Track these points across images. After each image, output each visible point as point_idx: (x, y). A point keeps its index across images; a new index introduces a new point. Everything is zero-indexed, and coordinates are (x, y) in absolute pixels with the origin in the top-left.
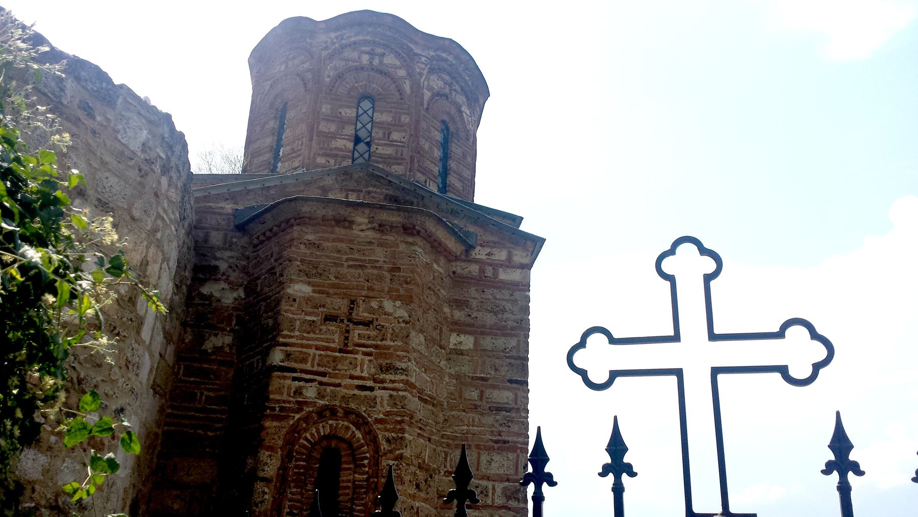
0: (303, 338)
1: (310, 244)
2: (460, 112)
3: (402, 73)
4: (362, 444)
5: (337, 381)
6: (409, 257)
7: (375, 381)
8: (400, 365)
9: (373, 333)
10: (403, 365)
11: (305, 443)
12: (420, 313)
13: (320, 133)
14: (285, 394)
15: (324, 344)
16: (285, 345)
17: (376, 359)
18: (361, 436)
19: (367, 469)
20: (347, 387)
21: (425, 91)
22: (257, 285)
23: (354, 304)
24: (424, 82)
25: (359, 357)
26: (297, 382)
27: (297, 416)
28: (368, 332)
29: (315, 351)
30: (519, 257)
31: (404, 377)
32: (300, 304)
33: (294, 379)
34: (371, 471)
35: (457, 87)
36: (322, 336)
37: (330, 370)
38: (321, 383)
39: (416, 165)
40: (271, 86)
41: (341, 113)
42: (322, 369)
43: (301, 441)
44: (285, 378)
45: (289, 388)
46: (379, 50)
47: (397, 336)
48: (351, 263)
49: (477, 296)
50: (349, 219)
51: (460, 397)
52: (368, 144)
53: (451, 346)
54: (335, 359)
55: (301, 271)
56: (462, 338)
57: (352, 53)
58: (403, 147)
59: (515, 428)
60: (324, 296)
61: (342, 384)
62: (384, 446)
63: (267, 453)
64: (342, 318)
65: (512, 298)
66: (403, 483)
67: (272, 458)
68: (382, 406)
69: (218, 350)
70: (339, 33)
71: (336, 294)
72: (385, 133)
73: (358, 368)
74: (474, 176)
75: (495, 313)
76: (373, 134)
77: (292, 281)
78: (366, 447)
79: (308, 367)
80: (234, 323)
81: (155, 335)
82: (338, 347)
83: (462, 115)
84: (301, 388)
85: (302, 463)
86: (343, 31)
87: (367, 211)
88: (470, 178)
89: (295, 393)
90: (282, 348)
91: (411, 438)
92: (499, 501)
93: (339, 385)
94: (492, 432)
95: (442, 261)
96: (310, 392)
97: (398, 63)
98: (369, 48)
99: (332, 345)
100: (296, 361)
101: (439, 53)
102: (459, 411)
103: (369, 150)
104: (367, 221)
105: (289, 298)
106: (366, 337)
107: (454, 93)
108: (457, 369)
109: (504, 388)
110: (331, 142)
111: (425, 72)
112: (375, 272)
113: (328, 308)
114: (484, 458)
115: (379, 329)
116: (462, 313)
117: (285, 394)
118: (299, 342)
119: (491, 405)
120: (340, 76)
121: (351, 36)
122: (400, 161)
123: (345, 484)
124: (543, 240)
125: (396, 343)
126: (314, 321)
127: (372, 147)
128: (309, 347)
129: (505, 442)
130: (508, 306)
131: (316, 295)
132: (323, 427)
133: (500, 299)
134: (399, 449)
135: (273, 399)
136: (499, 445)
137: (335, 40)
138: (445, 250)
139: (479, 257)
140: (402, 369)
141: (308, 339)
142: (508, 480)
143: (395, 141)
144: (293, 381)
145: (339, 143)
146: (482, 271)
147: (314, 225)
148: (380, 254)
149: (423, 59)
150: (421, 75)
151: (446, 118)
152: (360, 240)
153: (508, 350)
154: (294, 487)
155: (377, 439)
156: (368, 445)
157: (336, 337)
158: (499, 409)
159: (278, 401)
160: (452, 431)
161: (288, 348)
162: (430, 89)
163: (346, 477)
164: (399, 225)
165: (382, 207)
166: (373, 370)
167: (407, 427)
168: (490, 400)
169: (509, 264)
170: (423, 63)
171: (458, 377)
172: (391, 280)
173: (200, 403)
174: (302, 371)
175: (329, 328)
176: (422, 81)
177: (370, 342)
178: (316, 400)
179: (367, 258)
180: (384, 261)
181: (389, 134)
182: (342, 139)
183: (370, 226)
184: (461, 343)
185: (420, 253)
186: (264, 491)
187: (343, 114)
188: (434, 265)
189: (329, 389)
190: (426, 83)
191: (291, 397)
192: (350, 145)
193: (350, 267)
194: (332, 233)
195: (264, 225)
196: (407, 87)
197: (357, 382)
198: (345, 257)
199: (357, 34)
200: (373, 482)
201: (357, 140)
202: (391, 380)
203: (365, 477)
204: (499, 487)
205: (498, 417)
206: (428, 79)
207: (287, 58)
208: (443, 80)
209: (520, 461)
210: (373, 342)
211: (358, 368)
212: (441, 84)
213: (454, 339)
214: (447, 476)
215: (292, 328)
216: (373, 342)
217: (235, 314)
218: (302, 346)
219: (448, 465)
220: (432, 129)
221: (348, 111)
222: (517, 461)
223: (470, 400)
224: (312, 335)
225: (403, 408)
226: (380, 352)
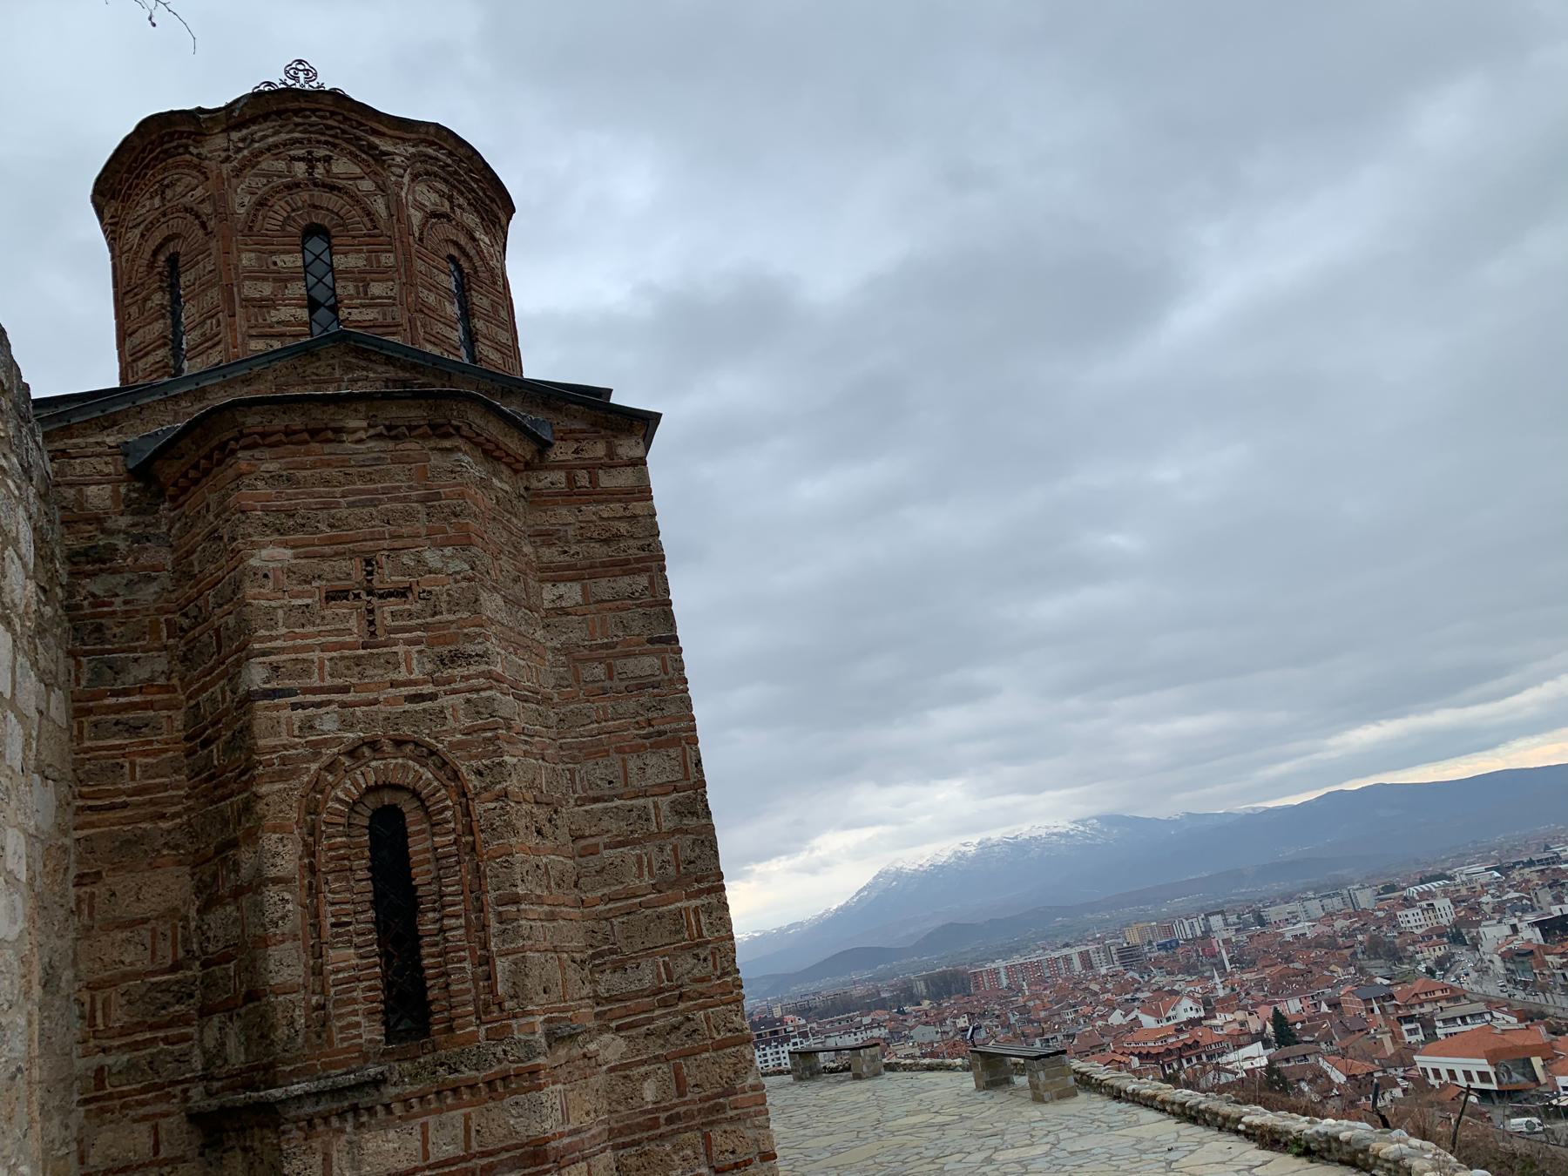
0: (295, 636)
1: (275, 478)
2: (474, 239)
4: (435, 787)
5: (372, 696)
6: (452, 472)
7: (435, 683)
8: (470, 648)
9: (417, 607)
10: (479, 649)
11: (337, 806)
12: (487, 560)
13: (248, 302)
14: (284, 734)
15: (334, 639)
16: (264, 653)
17: (431, 646)
18: (430, 776)
19: (452, 825)
20: (391, 702)
21: (412, 211)
22: (191, 564)
23: (372, 565)
24: (406, 198)
25: (400, 649)
26: (300, 711)
27: (314, 767)
28: (408, 607)
29: (322, 654)
30: (627, 449)
31: (484, 667)
32: (276, 580)
33: (294, 706)
34: (459, 827)
36: (329, 627)
37: (354, 681)
38: (343, 705)
39: (421, 331)
40: (142, 236)
41: (275, 263)
42: (339, 682)
43: (330, 804)
44: (277, 708)
45: (289, 723)
46: (322, 152)
47: (458, 604)
48: (351, 499)
49: (571, 520)
50: (332, 425)
51: (578, 681)
52: (334, 309)
53: (547, 605)
54: (358, 661)
55: (266, 525)
56: (562, 588)
57: (275, 163)
58: (394, 304)
59: (672, 709)
60: (316, 561)
61: (381, 699)
62: (473, 782)
63: (275, 837)
64: (356, 592)
65: (627, 513)
66: (516, 833)
67: (285, 842)
68: (456, 719)
70: (245, 132)
71: (337, 554)
72: (357, 287)
73: (403, 668)
74: (515, 339)
75: (606, 541)
76: (339, 291)
77: (254, 545)
78: (443, 791)
79: (315, 681)
80: (164, 634)
81: (19, 679)
82: (361, 641)
83: (479, 245)
84: (310, 719)
85: (339, 839)
86: (254, 128)
87: (362, 407)
88: (510, 343)
89: (300, 728)
90: (262, 659)
91: (515, 760)
93: (376, 702)
94: (637, 723)
95: (506, 472)
96: (328, 723)
97: (358, 171)
98: (303, 151)
99: (348, 639)
100: (290, 677)
101: (421, 148)
102: (579, 701)
103: (337, 319)
104: (364, 424)
105: (255, 574)
106: (406, 614)
107: (458, 211)
108: (563, 638)
109: (642, 654)
110: (269, 312)
111: (406, 179)
112: (399, 506)
113: (328, 580)
114: (633, 764)
115: (424, 599)
116: (554, 549)
117: (284, 734)
118: (290, 643)
119: (627, 683)
122: (394, 329)
123: (421, 857)
124: (661, 415)
125: (459, 615)
126: (307, 606)
127: (340, 313)
128: (310, 648)
129: (660, 734)
130: (623, 527)
131: (303, 561)
132: (363, 774)
133: (609, 519)
134: (500, 782)
135: (266, 747)
136: (652, 740)
137: (241, 145)
138: (508, 455)
139: (562, 458)
140: (477, 655)
141: (304, 637)
142: (676, 790)
143: (378, 298)
144: (292, 710)
145: (284, 313)
146: (571, 480)
147: (271, 446)
149: (398, 159)
150: (400, 185)
151: (454, 252)
152: (361, 457)
153: (637, 594)
154: (336, 880)
155: (460, 775)
156: (445, 786)
157: (353, 623)
158: (640, 687)
159: (274, 749)
160: (573, 734)
161: (273, 658)
162: (420, 207)
163: (417, 846)
164: (422, 423)
165: (387, 397)
166: (429, 667)
167: (506, 747)
168: (624, 676)
169: (612, 463)
170: (400, 166)
171: (565, 650)
172: (428, 514)
173: (133, 779)
174: (306, 691)
175: (337, 611)
176: (403, 194)
177: (414, 622)
178: (341, 734)
179: (380, 485)
180: (410, 487)
181: (366, 286)
182: (286, 306)
183: (372, 432)
184: (561, 596)
185: (468, 463)
186: (283, 899)
187: (280, 264)
188: (494, 480)
189: (358, 711)
190: (410, 197)
191: (294, 737)
192: (304, 314)
193: (351, 505)
194: (308, 454)
195: (182, 461)
196: (380, 206)
197: (405, 691)
198: (338, 490)
199: (276, 133)
200: (467, 843)
201: (313, 305)
202: (462, 677)
203: (452, 837)
204: (664, 802)
205: (642, 699)
206: (411, 191)
207: (162, 185)
208: (437, 191)
209: (688, 760)
210: (419, 621)
211: (403, 668)
212: (434, 197)
213: (548, 593)
214: (581, 805)
215: (272, 623)
216: (419, 621)
217: (162, 620)
218: (295, 649)
219: (579, 788)
220: (435, 270)
221: (287, 258)
222: (684, 756)
223: (594, 681)
224: (309, 629)
225: (492, 716)
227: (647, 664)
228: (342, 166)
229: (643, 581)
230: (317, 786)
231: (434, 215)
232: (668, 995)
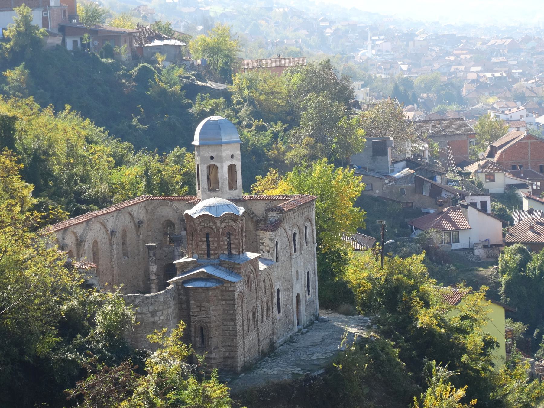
3: (214, 227)
35: (231, 221)
46: (208, 222)
69: (184, 308)
92: (232, 329)
96: (197, 318)
120: (201, 230)
121: (202, 219)
148: (204, 295)
169: (231, 286)
196: (215, 230)
213: (222, 302)
226: (206, 312)
227: (232, 312)
228: (211, 224)
229: (232, 302)
230: (195, 324)
231: (225, 227)
232: (229, 346)
